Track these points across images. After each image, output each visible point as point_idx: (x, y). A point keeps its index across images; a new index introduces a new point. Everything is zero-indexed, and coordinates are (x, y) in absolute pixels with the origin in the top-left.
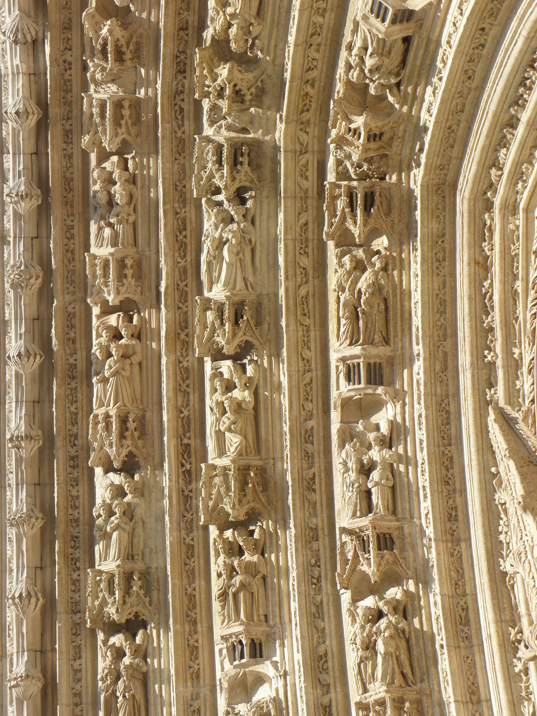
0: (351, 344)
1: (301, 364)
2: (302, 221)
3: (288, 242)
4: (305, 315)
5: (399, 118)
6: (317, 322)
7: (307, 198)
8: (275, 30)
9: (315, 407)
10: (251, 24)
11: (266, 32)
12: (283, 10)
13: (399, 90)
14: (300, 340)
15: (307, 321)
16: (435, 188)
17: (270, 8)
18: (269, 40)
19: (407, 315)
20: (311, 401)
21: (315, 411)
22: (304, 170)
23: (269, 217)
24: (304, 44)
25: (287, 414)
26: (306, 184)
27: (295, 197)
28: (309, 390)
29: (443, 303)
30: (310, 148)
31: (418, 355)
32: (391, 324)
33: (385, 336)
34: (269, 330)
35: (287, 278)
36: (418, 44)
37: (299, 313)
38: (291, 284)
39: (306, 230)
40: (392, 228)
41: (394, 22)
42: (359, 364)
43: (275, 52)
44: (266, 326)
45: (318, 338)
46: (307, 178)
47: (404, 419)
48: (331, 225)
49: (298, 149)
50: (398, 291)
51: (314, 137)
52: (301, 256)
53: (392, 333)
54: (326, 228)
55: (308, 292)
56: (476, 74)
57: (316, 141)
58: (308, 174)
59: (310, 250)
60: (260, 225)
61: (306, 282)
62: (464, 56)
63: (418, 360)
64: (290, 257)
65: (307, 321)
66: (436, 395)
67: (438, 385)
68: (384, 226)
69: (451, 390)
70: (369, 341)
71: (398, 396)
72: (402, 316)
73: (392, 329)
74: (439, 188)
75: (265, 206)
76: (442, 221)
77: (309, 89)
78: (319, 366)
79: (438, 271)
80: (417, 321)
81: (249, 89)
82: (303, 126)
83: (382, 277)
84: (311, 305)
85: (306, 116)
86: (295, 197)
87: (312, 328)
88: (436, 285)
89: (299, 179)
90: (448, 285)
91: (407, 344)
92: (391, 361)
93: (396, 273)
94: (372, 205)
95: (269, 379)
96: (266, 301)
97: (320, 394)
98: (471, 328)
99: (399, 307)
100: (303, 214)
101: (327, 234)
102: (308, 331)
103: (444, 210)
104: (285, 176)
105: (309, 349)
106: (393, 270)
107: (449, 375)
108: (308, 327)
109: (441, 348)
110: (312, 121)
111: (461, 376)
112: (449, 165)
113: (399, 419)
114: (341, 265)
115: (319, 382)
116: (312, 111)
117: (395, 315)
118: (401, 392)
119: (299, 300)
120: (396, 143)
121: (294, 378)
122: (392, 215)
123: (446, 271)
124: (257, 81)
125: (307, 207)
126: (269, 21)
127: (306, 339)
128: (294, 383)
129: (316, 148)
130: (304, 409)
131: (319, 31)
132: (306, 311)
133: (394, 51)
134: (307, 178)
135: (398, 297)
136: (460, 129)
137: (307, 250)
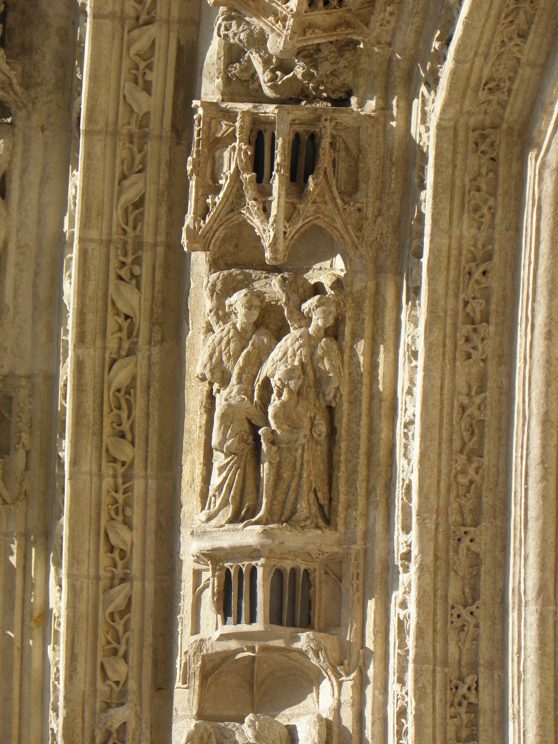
0: (235, 519)
1: (105, 559)
2: (130, 195)
3: (91, 246)
4: (123, 436)
6: (153, 456)
7: (144, 136)
9: (133, 674)
14: (106, 500)
15: (126, 452)
16: (473, 136)
19: (382, 453)
20: (125, 657)
21: (132, 685)
22: (142, 65)
23: (44, 180)
25: (61, 686)
26: (143, 103)
27: (115, 134)
28: (120, 628)
29: (476, 428)
31: (407, 556)
32: (342, 474)
33: (324, 502)
34: (27, 468)
35: (81, 339)
37: (107, 429)
38: (92, 355)
39: (139, 219)
40: (359, 229)
42: (253, 571)
44: (19, 457)
45: (152, 495)
47: (360, 719)
48: (203, 211)
49: (131, 13)
50: (365, 390)
52: (123, 286)
53: (342, 498)
54: (189, 219)
55: (134, 378)
58: (151, 76)
59: (145, 272)
60: (21, 200)
61: (131, 352)
63: (406, 569)
64: (92, 286)
65: (126, 452)
66: (445, 663)
67: (452, 636)
68: (339, 224)
69: (485, 651)
70: (283, 515)
71: (350, 661)
72: (370, 454)
73: (342, 487)
74: (484, 137)
75: (37, 151)
76: (486, 220)
78: (150, 568)
79: (468, 348)
80: (408, 469)
83: (326, 352)
84: (138, 412)
86: (115, 134)
87: (138, 470)
89: (128, 86)
90: (490, 384)
91: (379, 528)
92: (335, 568)
94: (310, 169)
95: (18, 592)
96: (23, 393)
97: (149, 640)
98: (544, 497)
99: (364, 431)
100: (134, 178)
101: (192, 235)
102: (127, 477)
103: (493, 193)
104: (93, 78)
105: (127, 523)
107: (481, 613)
108: (128, 466)
109: (466, 542)
111: (512, 617)
112: (511, 80)
113: (348, 719)
114: (223, 315)
115: (149, 609)
117: (354, 450)
118: (356, 649)
119: (109, 396)
121: (86, 595)
122: (360, 196)
123: (490, 347)
125: (143, 161)
127: (120, 497)
128: (82, 608)
129: (175, 14)
130: (105, 677)
132: (126, 427)
135: (364, 405)
137: (137, 270)
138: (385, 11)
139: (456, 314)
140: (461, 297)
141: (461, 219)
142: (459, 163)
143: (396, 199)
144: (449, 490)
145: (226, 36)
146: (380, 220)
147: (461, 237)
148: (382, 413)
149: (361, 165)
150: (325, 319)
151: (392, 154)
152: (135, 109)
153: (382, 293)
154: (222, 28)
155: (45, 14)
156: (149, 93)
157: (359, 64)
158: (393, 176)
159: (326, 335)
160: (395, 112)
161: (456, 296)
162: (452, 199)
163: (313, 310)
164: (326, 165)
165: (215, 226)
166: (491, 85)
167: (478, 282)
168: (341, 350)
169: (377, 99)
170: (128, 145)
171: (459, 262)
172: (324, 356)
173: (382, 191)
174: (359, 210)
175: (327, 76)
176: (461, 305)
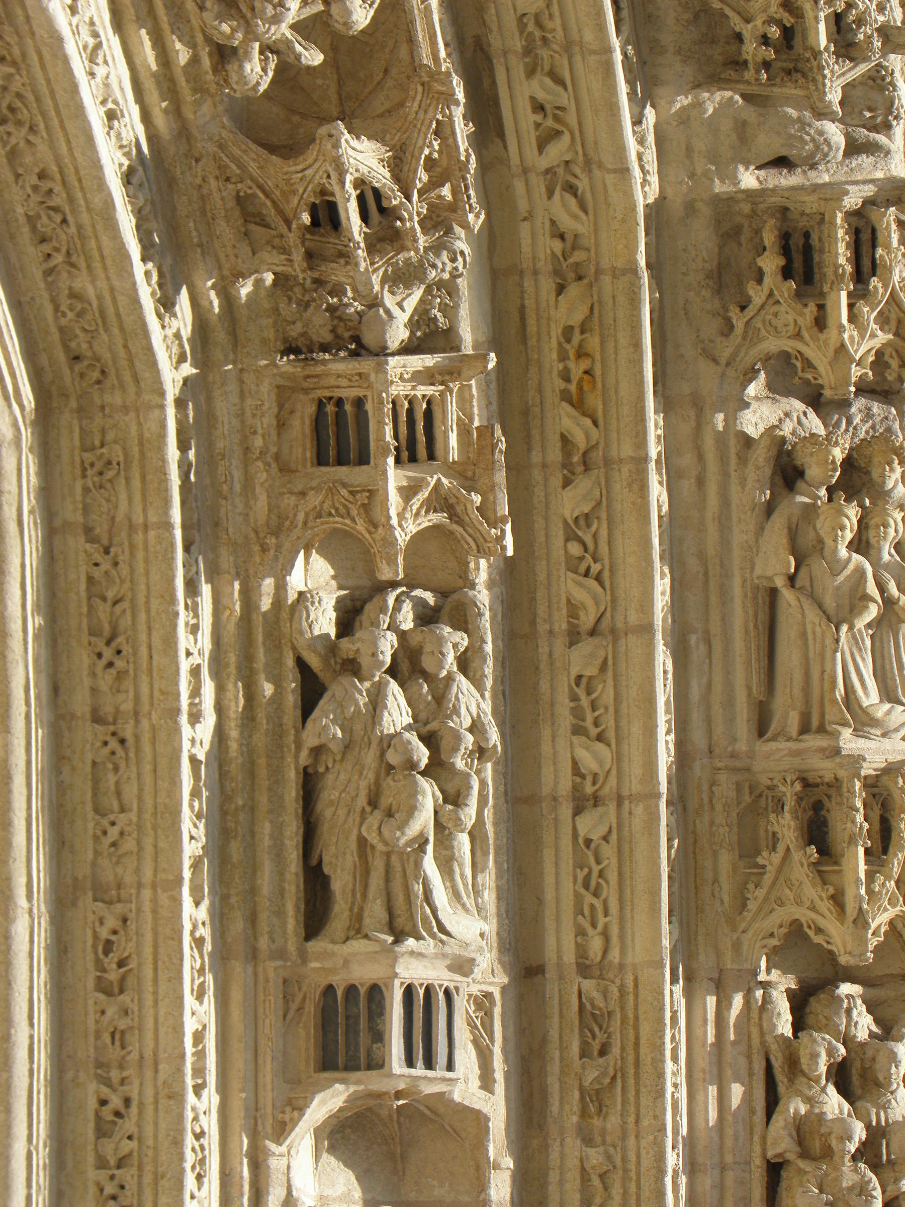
5: (279, 547)
7: (528, 51)
8: (711, 551)
10: (792, 579)
11: (740, 536)
12: (698, 651)
13: (301, 663)
16: (112, 379)
17: (738, 644)
18: (725, 503)
22: (550, 123)
24: (620, 625)
26: (540, 88)
27: (568, 47)
30: (539, 186)
36: (280, 913)
40: (222, 167)
41: (377, 994)
43: (701, 457)
46: (539, 108)
48: (444, 131)
51: (529, 217)
56: (93, 974)
57: (523, 205)
62: (148, 1053)
68: (253, 168)
77: (579, 431)
81: (771, 294)
82: (578, 256)
85: (569, 310)
88: (42, 148)
89: (564, 98)
93: (183, 55)
106: (195, 60)
110: (547, 285)
112: (86, 490)
116: (556, 332)
120: (268, 420)
124: (747, 323)
126: (737, 591)
129: (519, 186)
131: (581, 692)
133: (351, 859)
134: (539, 108)
136: (87, 682)
138: (263, 437)
139: (73, 211)
140: (73, 230)
141: (100, 298)
142: (122, 353)
143: (182, 211)
144: (24, 55)
145: (453, 260)
146: (198, 181)
147: (93, 282)
148: (132, 11)
149: (240, 222)
150: (242, 78)
151: (203, 254)
152: (548, 81)
153: (171, 116)
154: (460, 267)
155: (685, 62)
156: (533, 99)
157: (275, 322)
158: (194, 234)
159: (234, 50)
160: (212, 294)
161: (80, 227)
162: (118, 315)
163: (261, 77)
164: (291, 235)
165: (421, 115)
166: (110, 474)
167: (57, 250)
168: (208, 40)
169: (240, 298)
170: (549, 36)
171: (88, 259)
172: (232, 33)
173: (204, 213)
174: (228, 179)
175: (314, 300)
176: (70, 218)
